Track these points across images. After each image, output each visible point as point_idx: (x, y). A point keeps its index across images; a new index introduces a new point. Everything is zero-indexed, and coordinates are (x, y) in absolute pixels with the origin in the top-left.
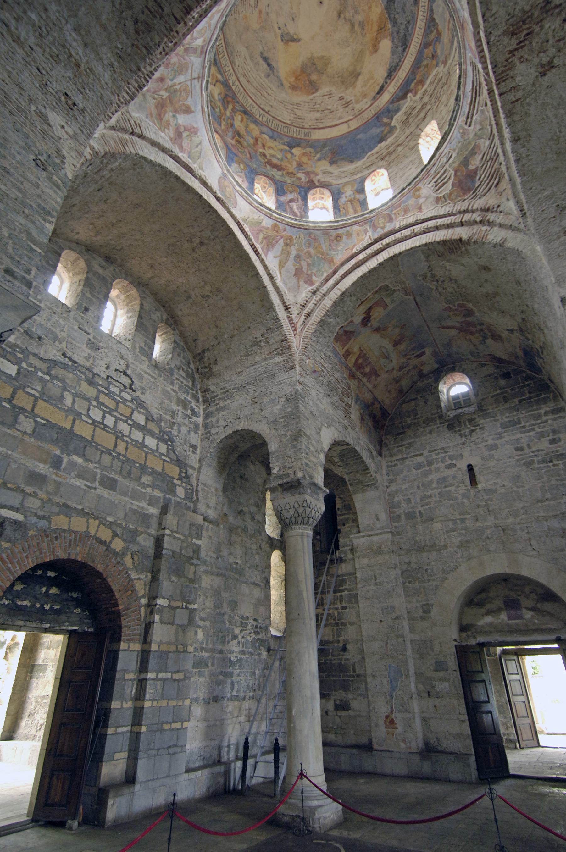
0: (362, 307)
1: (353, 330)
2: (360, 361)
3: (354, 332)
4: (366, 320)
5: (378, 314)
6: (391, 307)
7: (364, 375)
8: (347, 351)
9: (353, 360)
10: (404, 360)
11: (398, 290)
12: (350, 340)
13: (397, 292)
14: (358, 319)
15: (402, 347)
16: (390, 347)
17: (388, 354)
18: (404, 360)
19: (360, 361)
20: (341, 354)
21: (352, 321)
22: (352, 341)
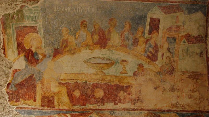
0: (9, 52)
1: (27, 76)
2: (77, 94)
3: (31, 77)
4: (31, 57)
5: (34, 42)
6: (39, 24)
7: (103, 101)
8: (44, 98)
9: (66, 99)
10: (141, 48)
11: (22, 7)
12: (35, 87)
13: (25, 9)
14: (20, 63)
15: (115, 39)
16: (98, 52)
17: (109, 59)
18: (141, 48)
19: (77, 94)
20: (38, 106)
21: (15, 71)
22: (39, 85)
